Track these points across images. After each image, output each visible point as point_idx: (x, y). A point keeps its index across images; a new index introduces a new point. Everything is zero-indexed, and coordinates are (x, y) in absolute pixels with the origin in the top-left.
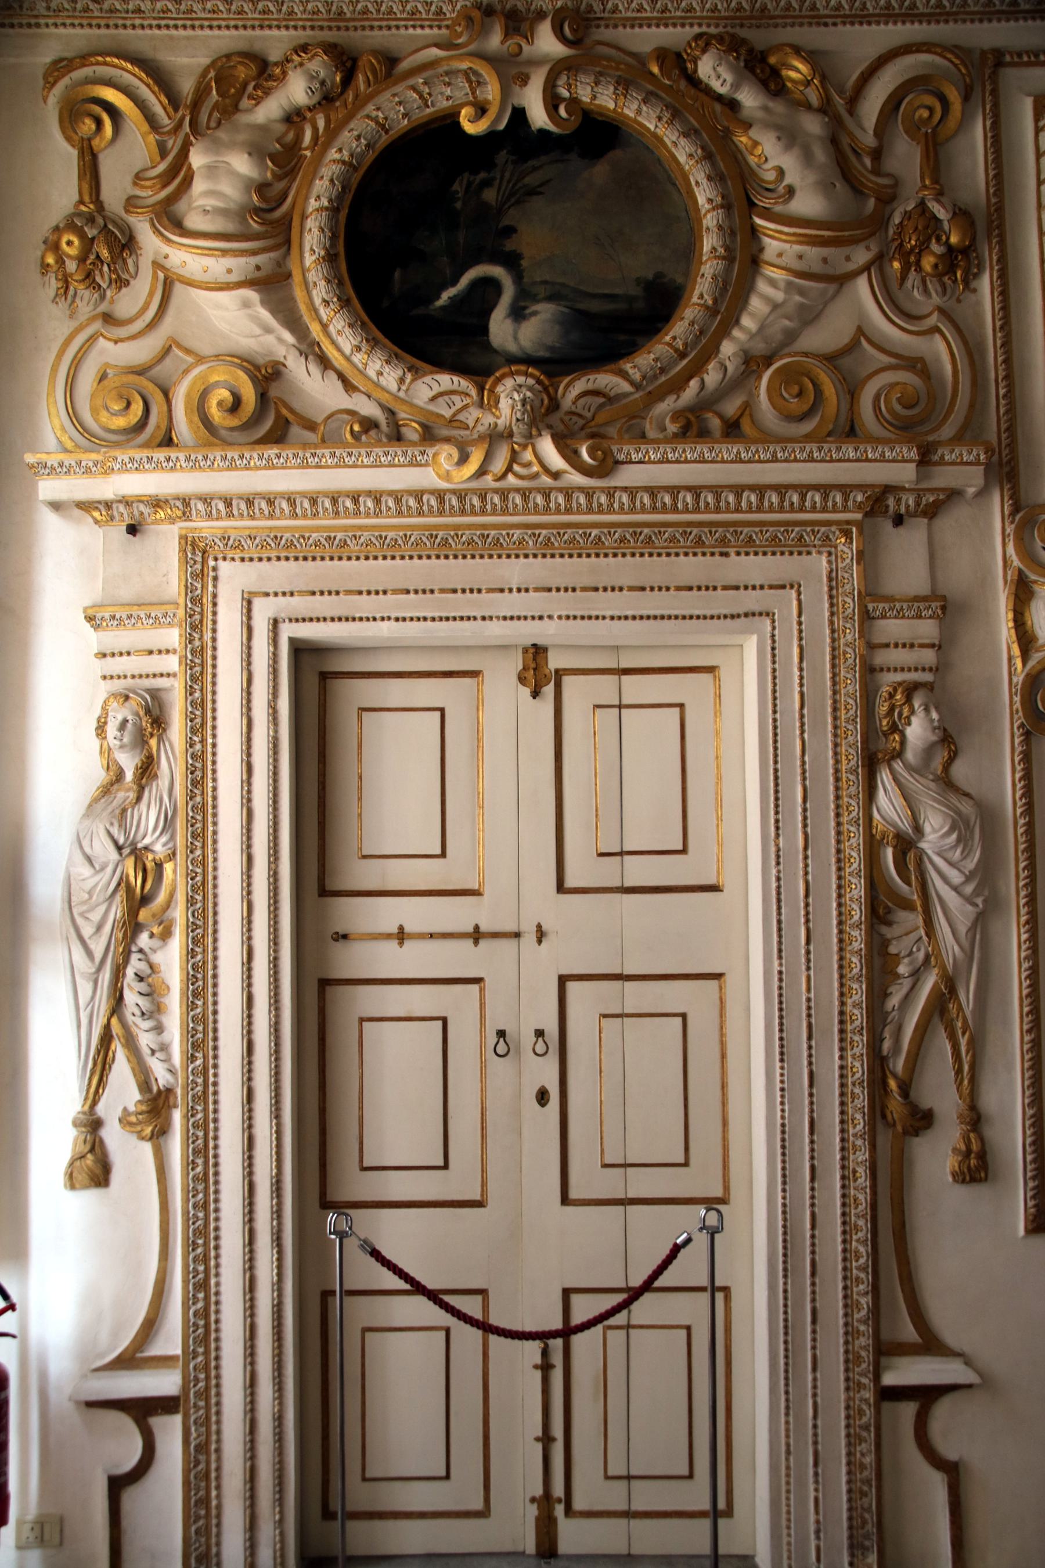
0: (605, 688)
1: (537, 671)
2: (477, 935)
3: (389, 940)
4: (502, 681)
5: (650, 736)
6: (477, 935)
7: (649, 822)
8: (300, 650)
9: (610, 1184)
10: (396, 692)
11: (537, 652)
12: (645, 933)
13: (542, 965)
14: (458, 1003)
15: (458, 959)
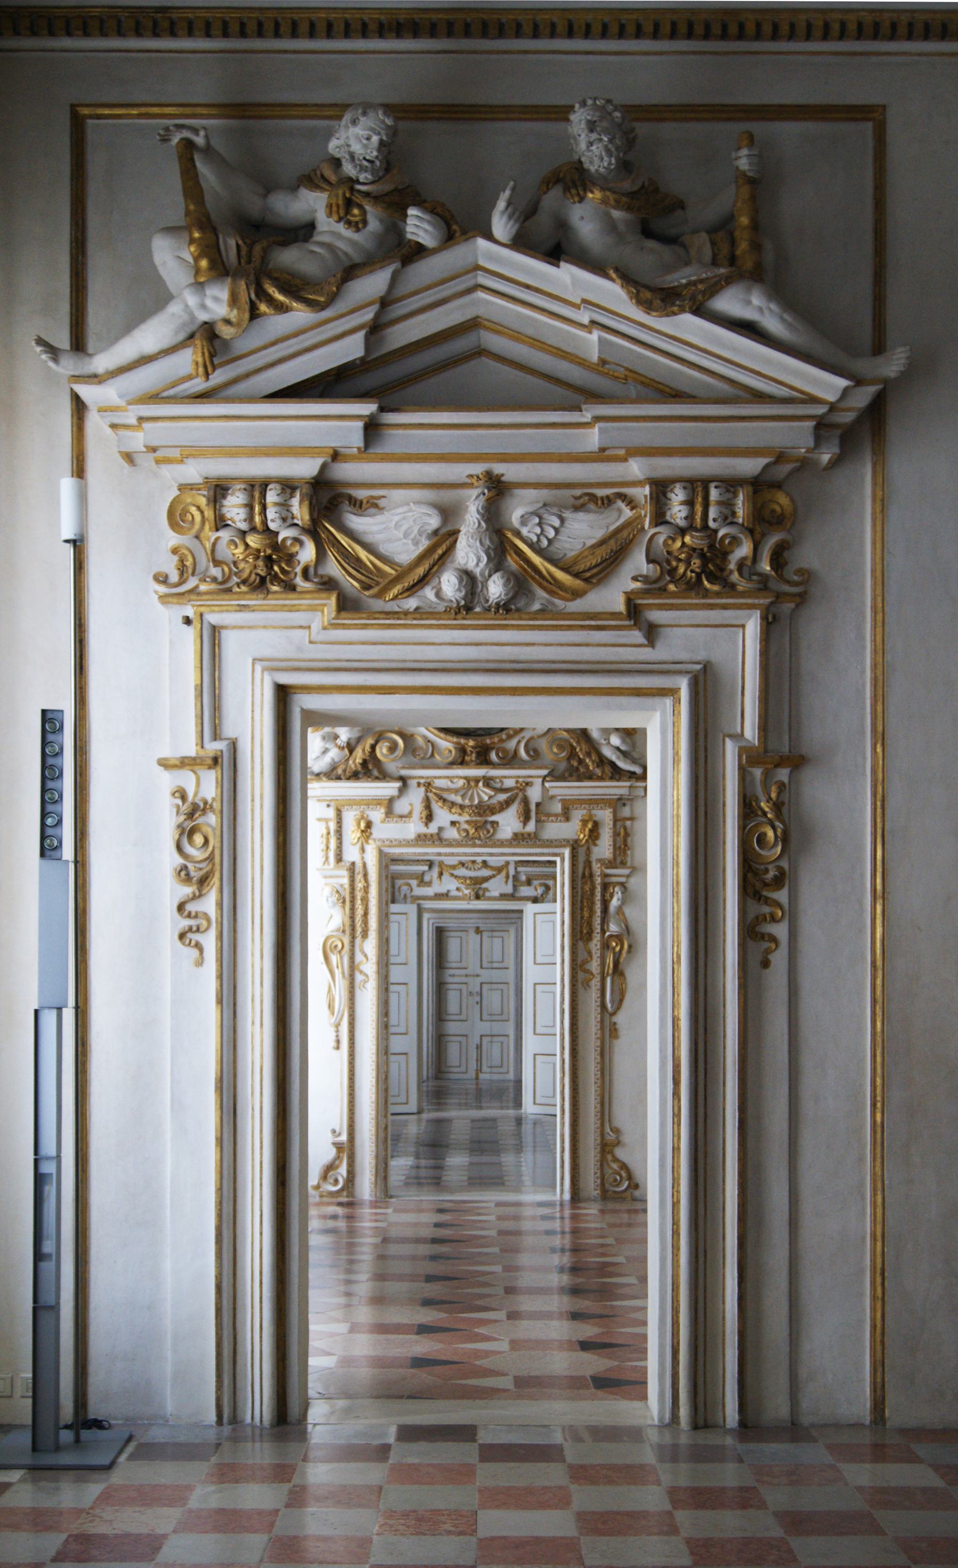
0: (490, 934)
1: (478, 931)
2: (467, 976)
3: (453, 976)
4: (472, 933)
5: (497, 942)
6: (467, 976)
7: (497, 956)
8: (437, 928)
9: (489, 1018)
10: (453, 934)
11: (478, 928)
12: (496, 975)
13: (479, 980)
14: (464, 987)
15: (464, 980)
